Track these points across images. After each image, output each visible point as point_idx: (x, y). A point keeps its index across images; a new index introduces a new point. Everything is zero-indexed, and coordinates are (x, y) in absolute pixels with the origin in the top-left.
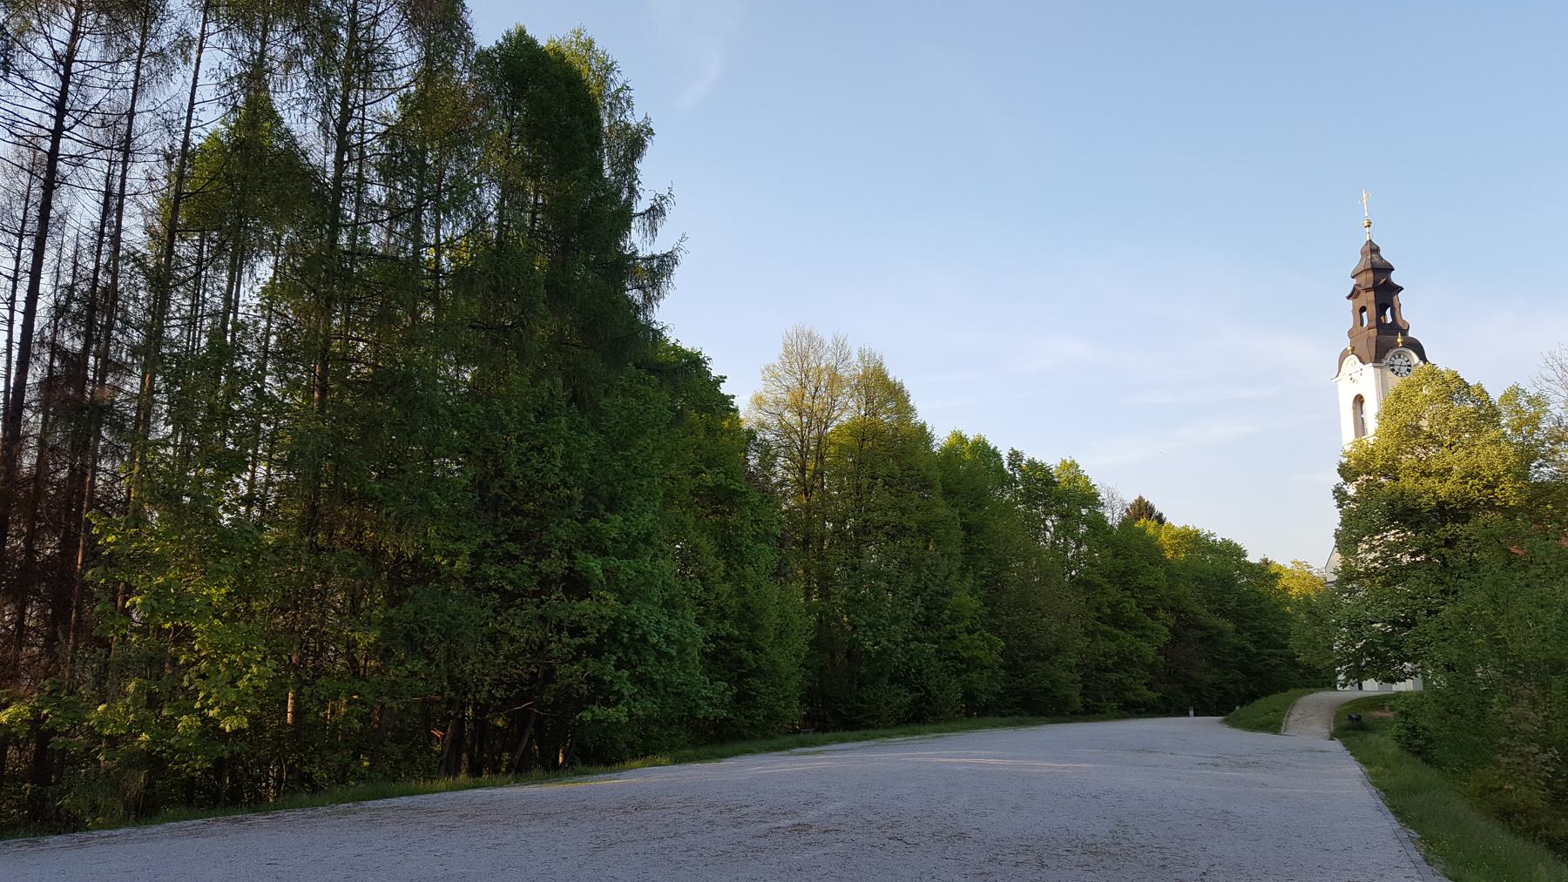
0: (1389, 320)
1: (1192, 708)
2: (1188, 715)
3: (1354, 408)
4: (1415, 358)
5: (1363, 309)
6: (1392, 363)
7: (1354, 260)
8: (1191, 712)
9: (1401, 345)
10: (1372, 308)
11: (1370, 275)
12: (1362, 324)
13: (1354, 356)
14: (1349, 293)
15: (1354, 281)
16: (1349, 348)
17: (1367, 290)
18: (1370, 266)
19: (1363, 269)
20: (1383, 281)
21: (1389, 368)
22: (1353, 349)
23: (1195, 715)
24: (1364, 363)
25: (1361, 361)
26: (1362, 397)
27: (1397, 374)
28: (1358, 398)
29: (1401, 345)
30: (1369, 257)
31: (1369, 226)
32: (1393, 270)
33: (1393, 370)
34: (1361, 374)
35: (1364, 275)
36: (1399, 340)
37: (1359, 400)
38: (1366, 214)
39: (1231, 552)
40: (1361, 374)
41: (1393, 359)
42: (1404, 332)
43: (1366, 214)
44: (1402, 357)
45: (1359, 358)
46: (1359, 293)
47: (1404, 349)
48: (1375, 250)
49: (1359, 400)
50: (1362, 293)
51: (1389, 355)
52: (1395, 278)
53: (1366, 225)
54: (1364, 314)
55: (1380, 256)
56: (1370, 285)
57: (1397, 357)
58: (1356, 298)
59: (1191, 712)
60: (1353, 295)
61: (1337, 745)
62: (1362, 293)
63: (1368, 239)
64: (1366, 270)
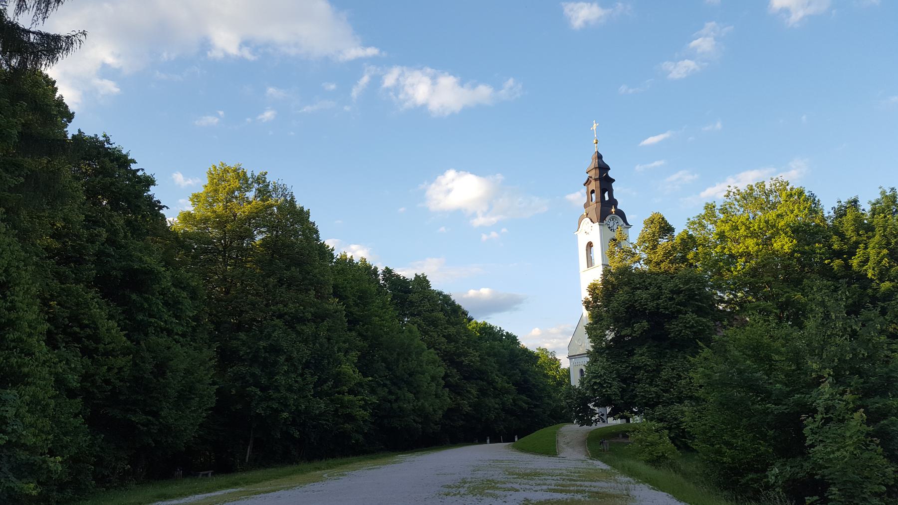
0: (607, 198)
1: (489, 437)
2: (485, 442)
3: (587, 250)
4: (622, 222)
5: (593, 192)
6: (608, 223)
7: (589, 162)
8: (488, 441)
9: (614, 213)
10: (598, 191)
11: (598, 171)
12: (592, 201)
13: (588, 220)
14: (585, 181)
15: (588, 175)
16: (585, 214)
17: (596, 180)
18: (597, 166)
19: (593, 167)
20: (604, 175)
21: (607, 227)
22: (587, 214)
23: (490, 443)
24: (593, 223)
25: (592, 221)
26: (592, 243)
27: (611, 230)
28: (589, 246)
29: (614, 213)
30: (597, 161)
31: (597, 143)
32: (610, 169)
33: (609, 228)
34: (591, 230)
35: (594, 170)
36: (613, 210)
37: (590, 245)
38: (595, 136)
39: (513, 339)
40: (591, 230)
41: (609, 221)
42: (616, 207)
43: (595, 136)
44: (614, 220)
45: (591, 220)
46: (591, 181)
47: (616, 216)
48: (600, 157)
49: (590, 245)
50: (593, 182)
51: (607, 219)
52: (611, 174)
53: (595, 142)
54: (593, 195)
55: (604, 162)
56: (598, 177)
57: (611, 220)
58: (589, 184)
59: (488, 441)
60: (587, 183)
61: (600, 465)
62: (593, 182)
63: (596, 151)
64: (595, 168)
